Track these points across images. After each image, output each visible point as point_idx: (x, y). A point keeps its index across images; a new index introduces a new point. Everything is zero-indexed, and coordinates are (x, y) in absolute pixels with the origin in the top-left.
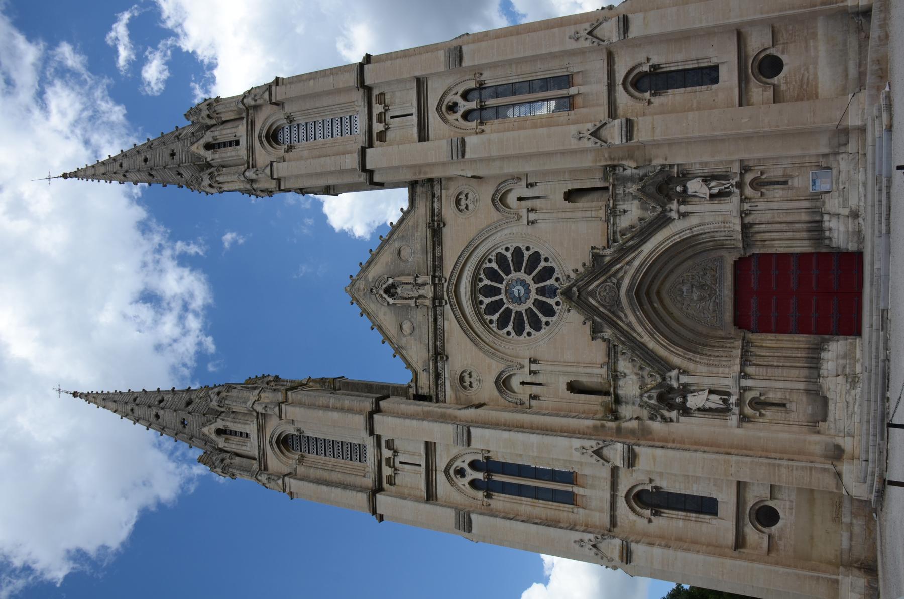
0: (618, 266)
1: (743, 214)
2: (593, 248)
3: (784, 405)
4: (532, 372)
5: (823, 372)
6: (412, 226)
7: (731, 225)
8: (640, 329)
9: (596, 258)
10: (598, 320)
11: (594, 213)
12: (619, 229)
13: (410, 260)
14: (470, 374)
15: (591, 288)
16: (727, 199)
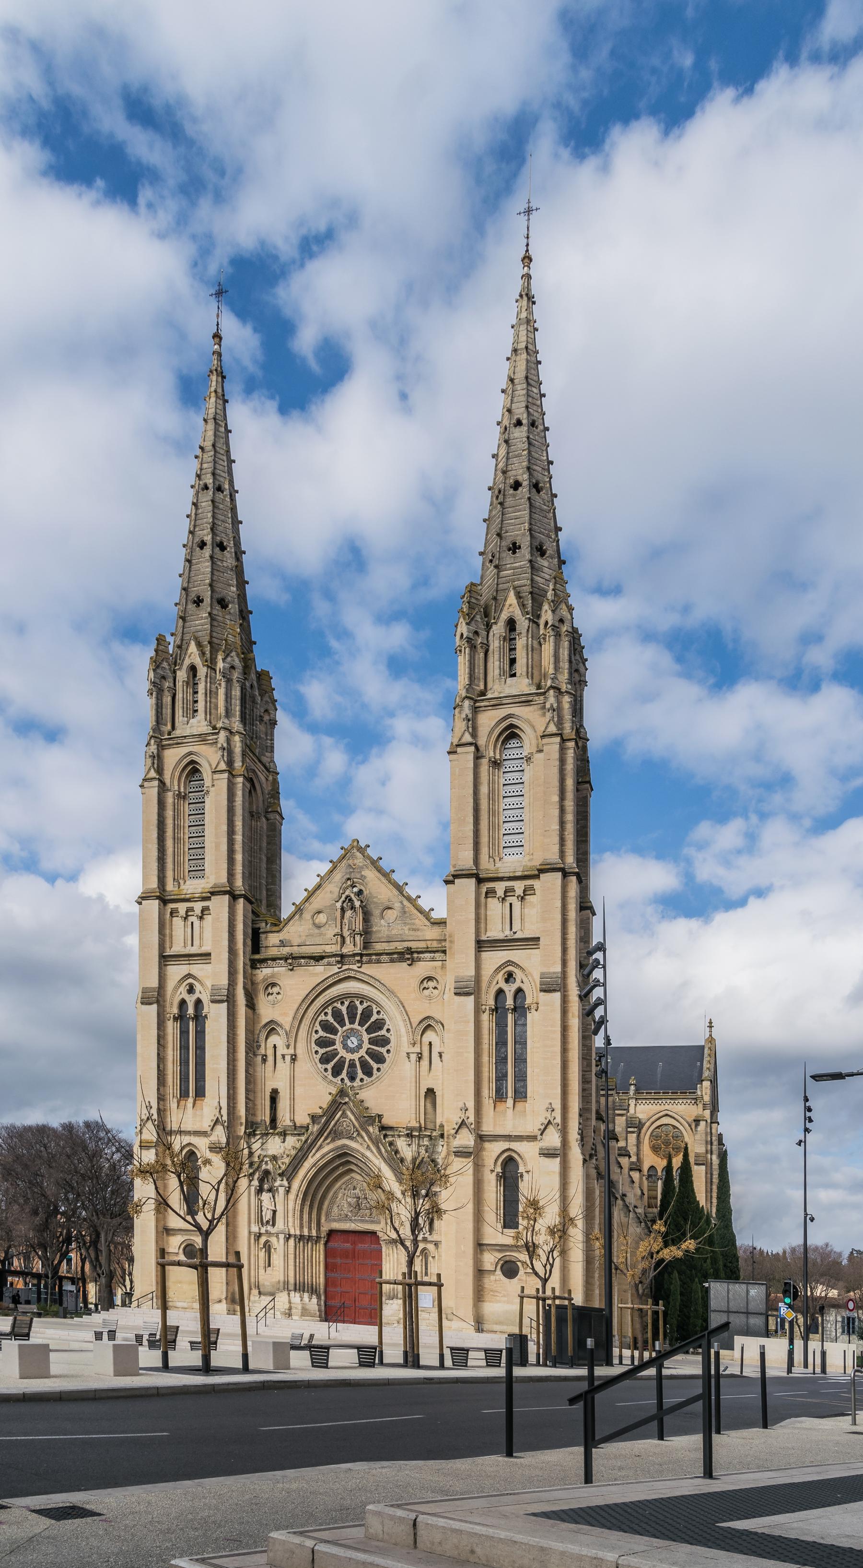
0: (366, 1138)
3: (269, 1265)
4: (283, 1056)
6: (414, 924)
8: (318, 1155)
13: (382, 921)
14: (278, 993)
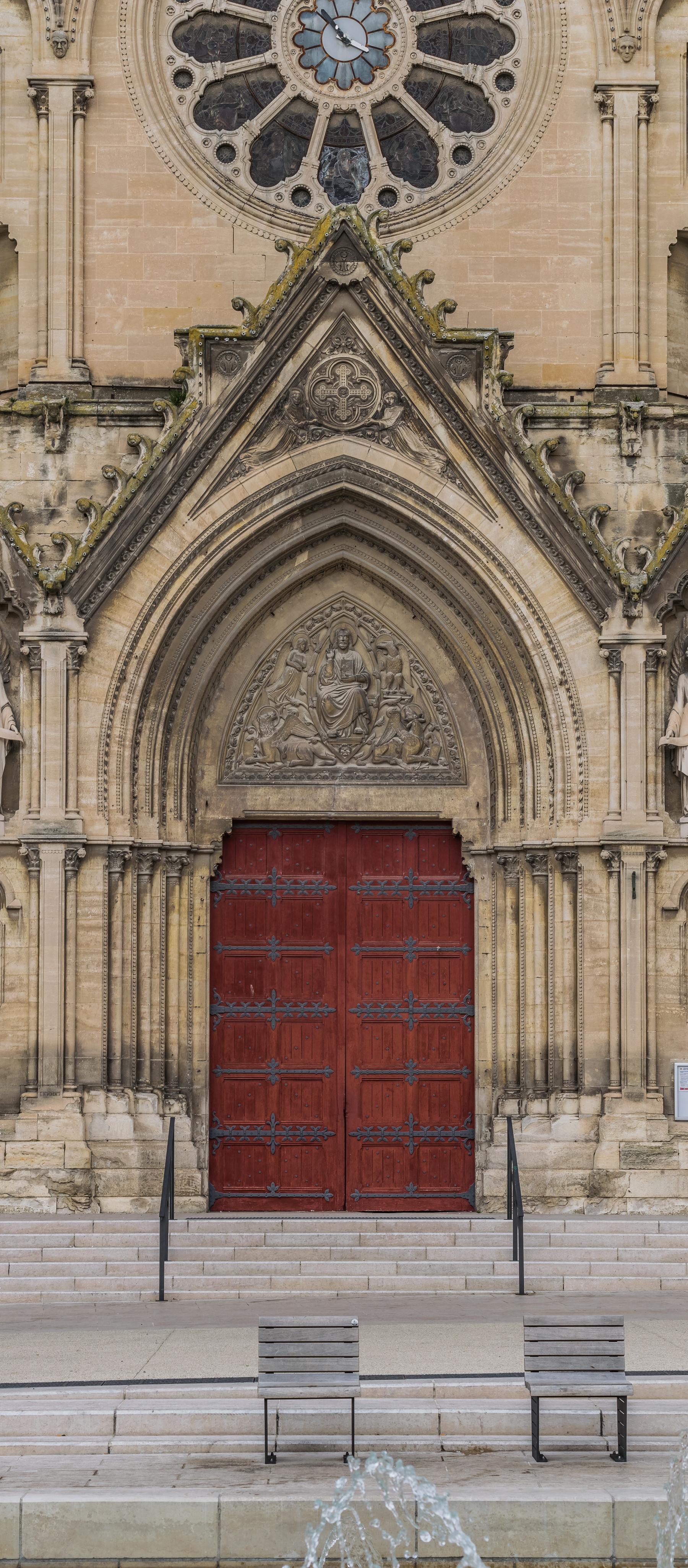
0: (441, 432)
1: (610, 852)
2: (505, 339)
5: (97, 1101)
7: (574, 814)
8: (223, 504)
9: (475, 353)
10: (252, 359)
11: (627, 342)
12: (571, 435)
15: (363, 327)
16: (657, 803)
